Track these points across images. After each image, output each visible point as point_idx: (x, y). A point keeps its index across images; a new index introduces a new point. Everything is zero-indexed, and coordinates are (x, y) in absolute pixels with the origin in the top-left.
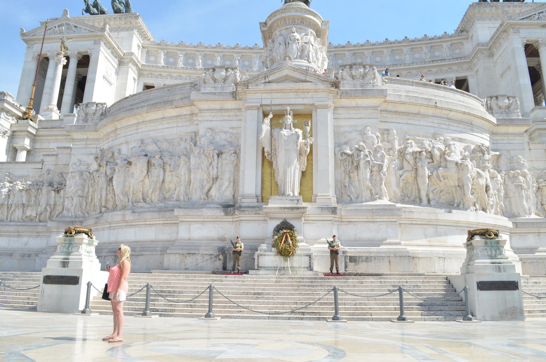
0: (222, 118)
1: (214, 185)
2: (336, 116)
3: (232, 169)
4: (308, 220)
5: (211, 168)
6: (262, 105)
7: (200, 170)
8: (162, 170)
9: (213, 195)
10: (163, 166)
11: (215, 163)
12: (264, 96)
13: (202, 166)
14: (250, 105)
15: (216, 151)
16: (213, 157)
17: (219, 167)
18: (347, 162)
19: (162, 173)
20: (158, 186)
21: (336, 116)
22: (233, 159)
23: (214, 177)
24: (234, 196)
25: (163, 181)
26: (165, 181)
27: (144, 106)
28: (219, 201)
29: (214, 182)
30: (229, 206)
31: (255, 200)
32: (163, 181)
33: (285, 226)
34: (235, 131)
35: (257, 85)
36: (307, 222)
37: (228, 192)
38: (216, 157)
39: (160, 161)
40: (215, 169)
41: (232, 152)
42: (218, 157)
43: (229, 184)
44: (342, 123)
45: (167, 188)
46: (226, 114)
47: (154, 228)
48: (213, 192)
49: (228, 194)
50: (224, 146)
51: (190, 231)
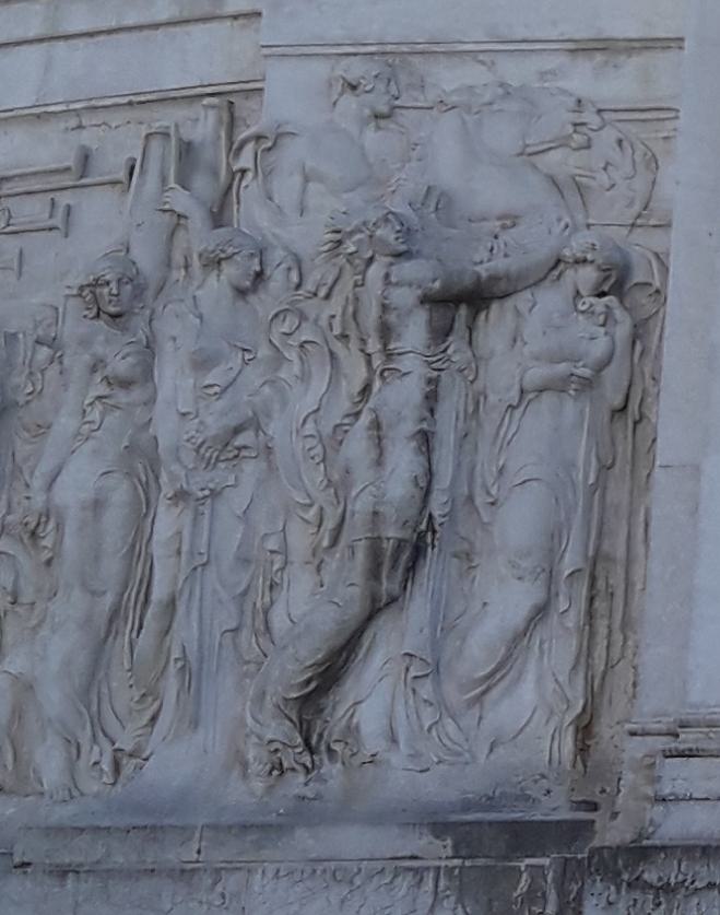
3: (581, 450)
5: (357, 445)
11: (402, 396)
16: (386, 332)
22: (599, 348)
23: (392, 532)
24: (585, 730)
28: (439, 787)
29: (387, 586)
30: (524, 837)
34: (619, 85)
37: (527, 692)
38: (414, 332)
40: (403, 460)
41: (587, 276)
42: (440, 333)
43: (541, 612)
49: (527, 721)
50: (510, 220)
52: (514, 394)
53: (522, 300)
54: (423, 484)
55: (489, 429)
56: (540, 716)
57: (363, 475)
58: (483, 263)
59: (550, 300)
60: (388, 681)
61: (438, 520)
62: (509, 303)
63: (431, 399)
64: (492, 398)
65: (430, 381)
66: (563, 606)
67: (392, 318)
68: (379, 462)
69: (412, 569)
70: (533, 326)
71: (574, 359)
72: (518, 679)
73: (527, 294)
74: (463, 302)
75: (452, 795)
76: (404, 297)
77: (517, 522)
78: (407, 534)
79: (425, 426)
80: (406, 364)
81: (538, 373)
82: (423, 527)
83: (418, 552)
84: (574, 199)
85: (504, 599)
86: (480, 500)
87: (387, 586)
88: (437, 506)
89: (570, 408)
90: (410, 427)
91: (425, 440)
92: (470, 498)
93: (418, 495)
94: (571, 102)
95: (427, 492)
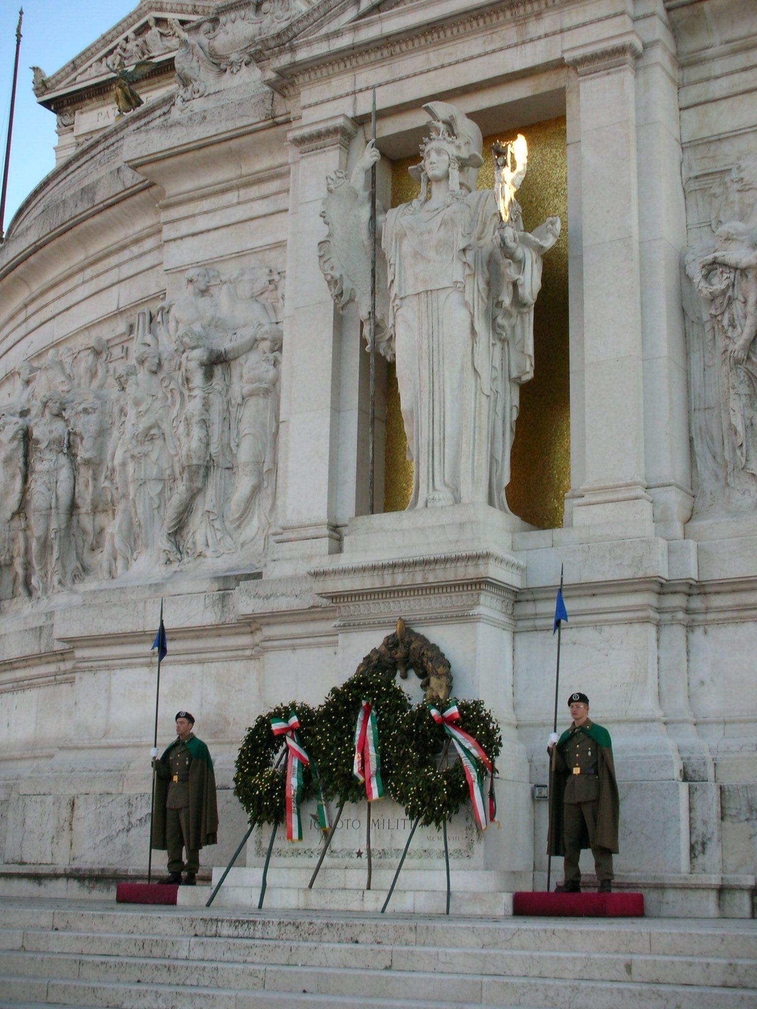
0: (239, 213)
1: (199, 500)
2: (694, 94)
4: (536, 616)
6: (361, 121)
7: (159, 442)
8: (63, 460)
9: (200, 539)
10: (69, 447)
11: (194, 406)
12: (366, 77)
13: (165, 426)
14: (306, 131)
15: (199, 355)
17: (215, 416)
18: (737, 306)
19: (65, 473)
20: (57, 522)
21: (694, 94)
25: (73, 507)
26: (79, 501)
27: (28, 229)
31: (324, 544)
32: (73, 507)
33: (400, 654)
35: (328, 37)
36: (529, 623)
37: (255, 522)
38: (198, 379)
39: (59, 428)
40: (197, 432)
41: (266, 345)
42: (209, 375)
44: (723, 119)
45: (89, 527)
46: (254, 191)
47: (32, 694)
48: (199, 530)
51: (109, 699)
52: (239, 400)
53: (241, 360)
54: (205, 440)
55: (233, 415)
56: (261, 531)
57: (184, 440)
58: (225, 344)
59: (253, 358)
60: (203, 524)
61: (213, 455)
62: (237, 361)
63: (206, 406)
64: (233, 402)
65: (204, 398)
66: (266, 485)
67: (189, 375)
68: (188, 435)
69: (206, 476)
70: (245, 371)
71: (260, 380)
72: (252, 517)
73: (244, 357)
74: (217, 363)
75: (225, 566)
76: (193, 365)
77: (244, 454)
78: (201, 462)
79: (203, 417)
80: (195, 392)
81: (247, 388)
82: (208, 458)
83: (207, 468)
84: (271, 313)
85: (244, 484)
86: (233, 445)
87: (198, 484)
88: (213, 449)
89: (261, 401)
90: (197, 418)
91: (205, 423)
92: (229, 444)
93: (203, 446)
94: (267, 271)
95: (208, 445)
